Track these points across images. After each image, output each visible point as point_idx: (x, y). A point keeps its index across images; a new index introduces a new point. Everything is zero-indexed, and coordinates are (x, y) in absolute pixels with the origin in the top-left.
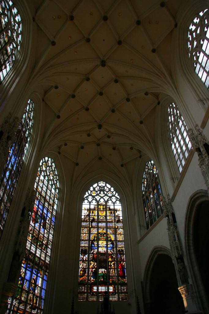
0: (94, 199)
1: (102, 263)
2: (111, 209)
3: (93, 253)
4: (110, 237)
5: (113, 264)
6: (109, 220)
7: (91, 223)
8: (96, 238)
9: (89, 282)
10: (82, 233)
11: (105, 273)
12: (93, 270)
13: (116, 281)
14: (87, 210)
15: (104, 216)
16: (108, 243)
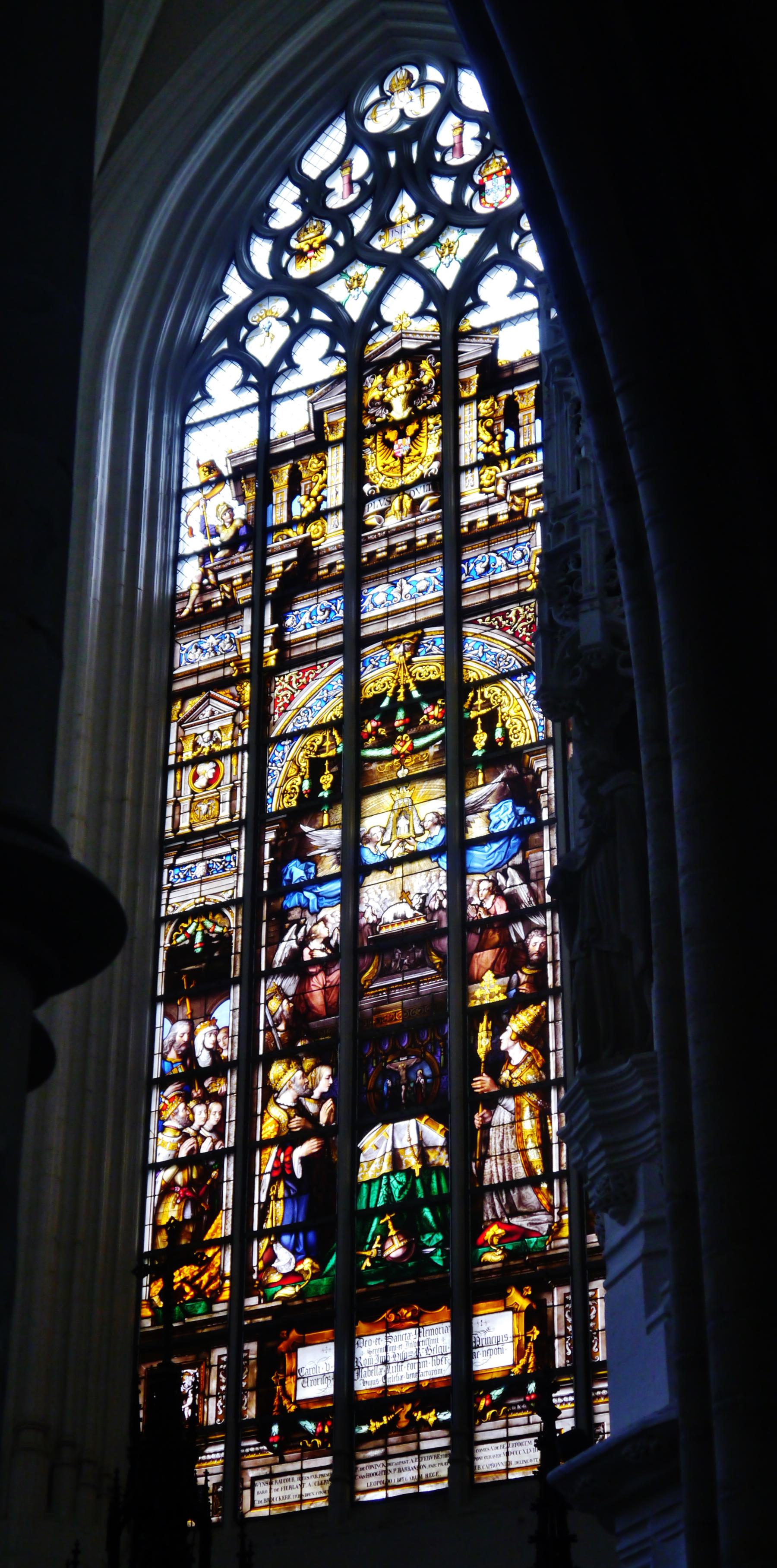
0: (318, 315)
1: (398, 1053)
2: (512, 366)
3: (296, 955)
4: (490, 720)
5: (522, 1038)
6: (481, 516)
7: (279, 617)
8: (327, 779)
9: (252, 1302)
10: (180, 766)
11: (428, 1168)
12: (300, 1152)
13: (554, 1233)
14: (238, 475)
15: (422, 480)
16: (472, 797)
